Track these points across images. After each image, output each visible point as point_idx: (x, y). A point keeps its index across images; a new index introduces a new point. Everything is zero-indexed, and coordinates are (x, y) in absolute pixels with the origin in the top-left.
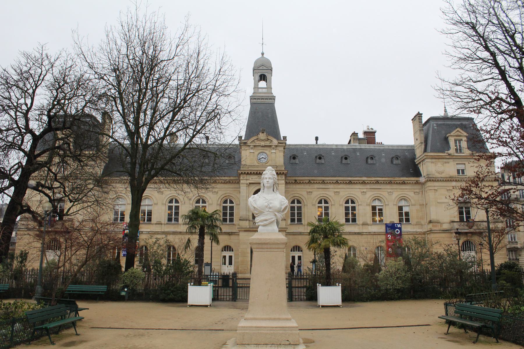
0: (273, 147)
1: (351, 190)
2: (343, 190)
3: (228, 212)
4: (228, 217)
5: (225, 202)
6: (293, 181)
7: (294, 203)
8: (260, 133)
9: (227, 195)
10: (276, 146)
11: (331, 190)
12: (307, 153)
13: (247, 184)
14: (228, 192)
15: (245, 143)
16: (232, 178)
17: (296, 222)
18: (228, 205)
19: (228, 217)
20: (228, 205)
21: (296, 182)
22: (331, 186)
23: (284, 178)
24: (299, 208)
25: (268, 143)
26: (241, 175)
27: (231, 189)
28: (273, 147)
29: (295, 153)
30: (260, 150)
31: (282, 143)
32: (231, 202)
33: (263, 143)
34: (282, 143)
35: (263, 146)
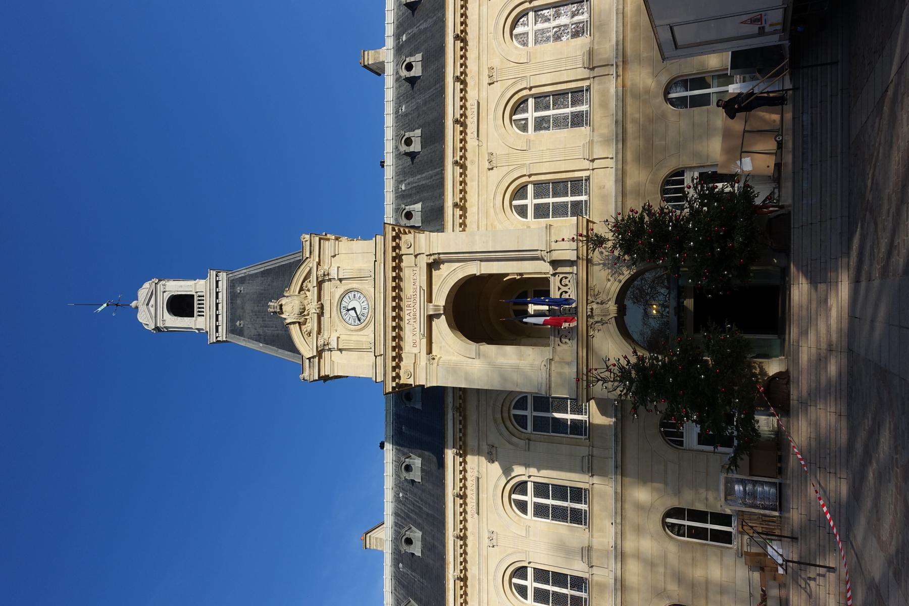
1: (484, 31)
2: (484, 58)
5: (522, 421)
11: (484, 94)
12: (401, 182)
17: (583, 198)
20: (529, 413)
22: (472, 94)
24: (541, 189)
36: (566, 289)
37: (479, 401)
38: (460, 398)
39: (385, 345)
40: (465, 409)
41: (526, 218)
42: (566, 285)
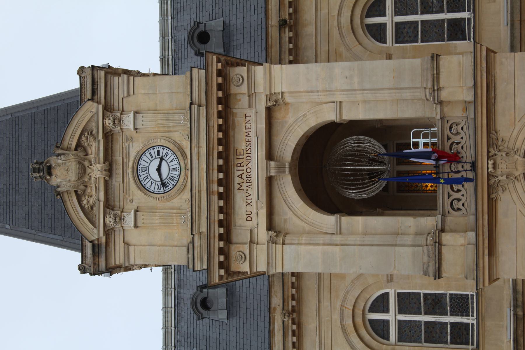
0: (109, 122)
3: (422, 318)
4: (448, 319)
6: (288, 34)
7: (383, 26)
8: (55, 181)
9: (349, 322)
10: (108, 108)
13: (272, 241)
14: (336, 316)
15: (96, 248)
16: (277, 301)
18: (392, 317)
19: (448, 319)
20: (392, 317)
21: (291, 23)
23: (243, 71)
25: (96, 148)
26: (234, 267)
27: (326, 303)
28: (109, 122)
29: (184, 36)
30: (125, 182)
31: (94, 83)
32: (381, 304)
33: (97, 171)
34: (94, 83)
35: (110, 171)
36: (457, 139)
37: (320, 301)
38: (293, 299)
39: (208, 218)
40: (299, 314)
41: (385, 43)
42: (458, 133)
